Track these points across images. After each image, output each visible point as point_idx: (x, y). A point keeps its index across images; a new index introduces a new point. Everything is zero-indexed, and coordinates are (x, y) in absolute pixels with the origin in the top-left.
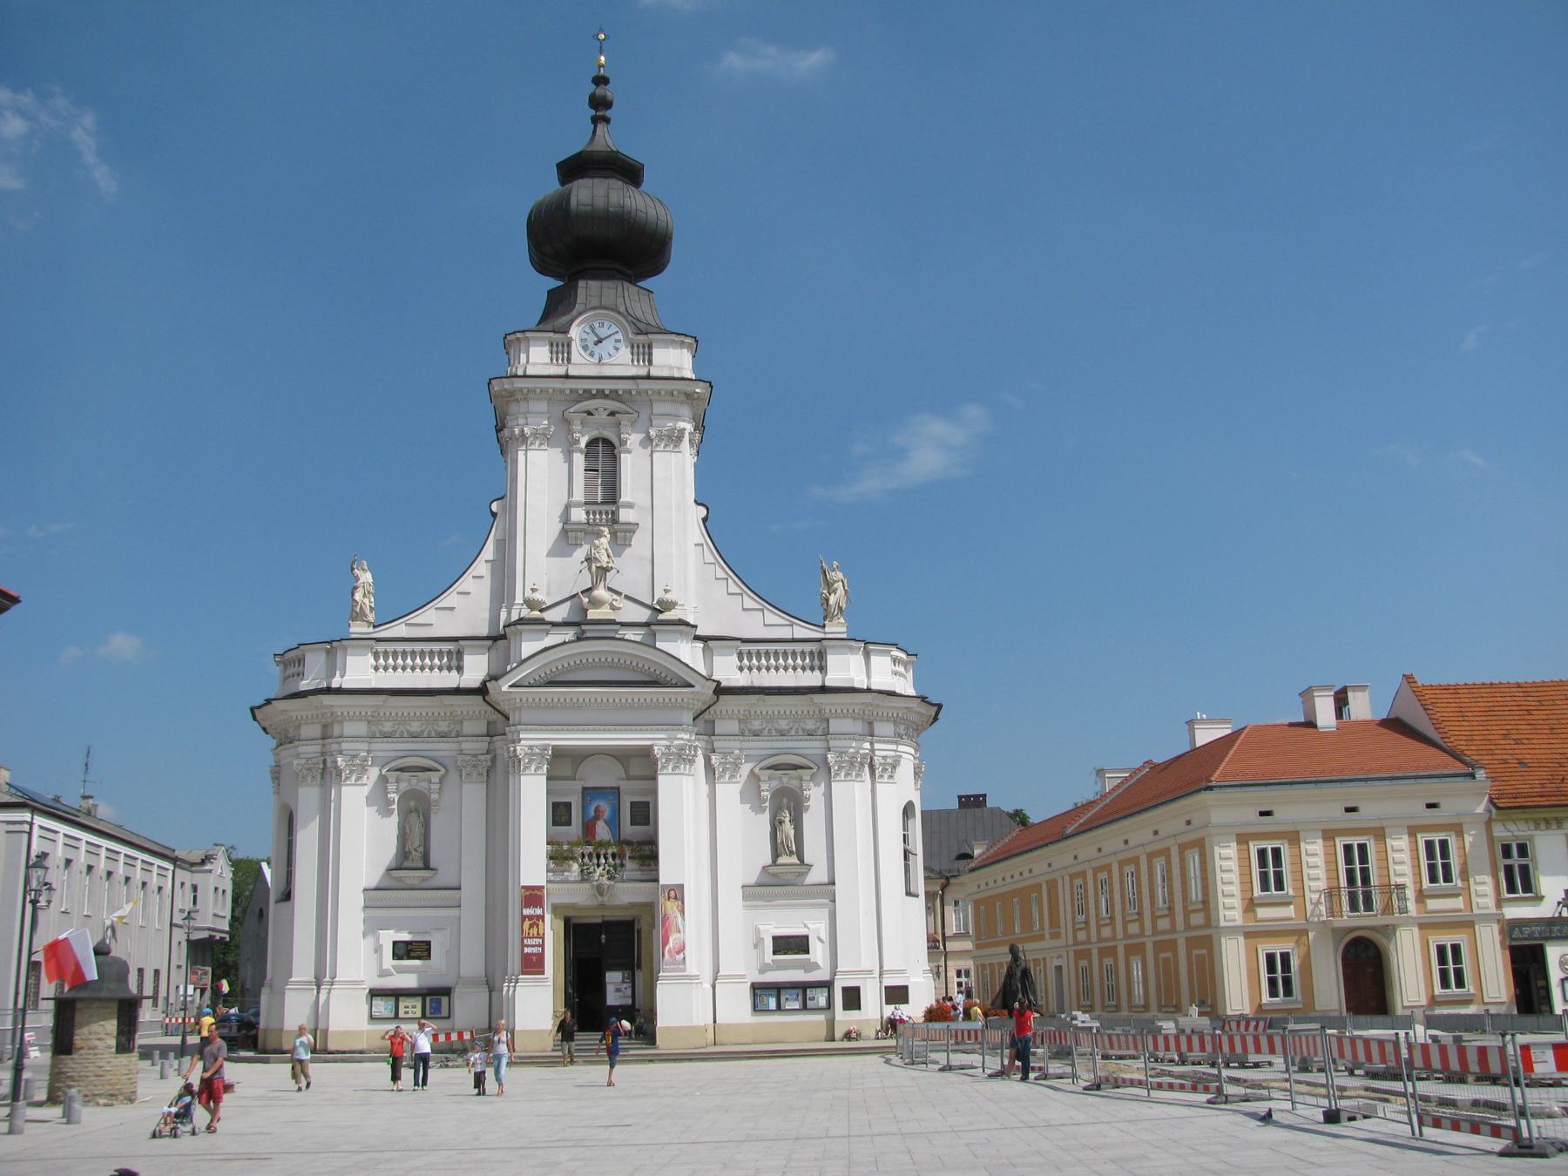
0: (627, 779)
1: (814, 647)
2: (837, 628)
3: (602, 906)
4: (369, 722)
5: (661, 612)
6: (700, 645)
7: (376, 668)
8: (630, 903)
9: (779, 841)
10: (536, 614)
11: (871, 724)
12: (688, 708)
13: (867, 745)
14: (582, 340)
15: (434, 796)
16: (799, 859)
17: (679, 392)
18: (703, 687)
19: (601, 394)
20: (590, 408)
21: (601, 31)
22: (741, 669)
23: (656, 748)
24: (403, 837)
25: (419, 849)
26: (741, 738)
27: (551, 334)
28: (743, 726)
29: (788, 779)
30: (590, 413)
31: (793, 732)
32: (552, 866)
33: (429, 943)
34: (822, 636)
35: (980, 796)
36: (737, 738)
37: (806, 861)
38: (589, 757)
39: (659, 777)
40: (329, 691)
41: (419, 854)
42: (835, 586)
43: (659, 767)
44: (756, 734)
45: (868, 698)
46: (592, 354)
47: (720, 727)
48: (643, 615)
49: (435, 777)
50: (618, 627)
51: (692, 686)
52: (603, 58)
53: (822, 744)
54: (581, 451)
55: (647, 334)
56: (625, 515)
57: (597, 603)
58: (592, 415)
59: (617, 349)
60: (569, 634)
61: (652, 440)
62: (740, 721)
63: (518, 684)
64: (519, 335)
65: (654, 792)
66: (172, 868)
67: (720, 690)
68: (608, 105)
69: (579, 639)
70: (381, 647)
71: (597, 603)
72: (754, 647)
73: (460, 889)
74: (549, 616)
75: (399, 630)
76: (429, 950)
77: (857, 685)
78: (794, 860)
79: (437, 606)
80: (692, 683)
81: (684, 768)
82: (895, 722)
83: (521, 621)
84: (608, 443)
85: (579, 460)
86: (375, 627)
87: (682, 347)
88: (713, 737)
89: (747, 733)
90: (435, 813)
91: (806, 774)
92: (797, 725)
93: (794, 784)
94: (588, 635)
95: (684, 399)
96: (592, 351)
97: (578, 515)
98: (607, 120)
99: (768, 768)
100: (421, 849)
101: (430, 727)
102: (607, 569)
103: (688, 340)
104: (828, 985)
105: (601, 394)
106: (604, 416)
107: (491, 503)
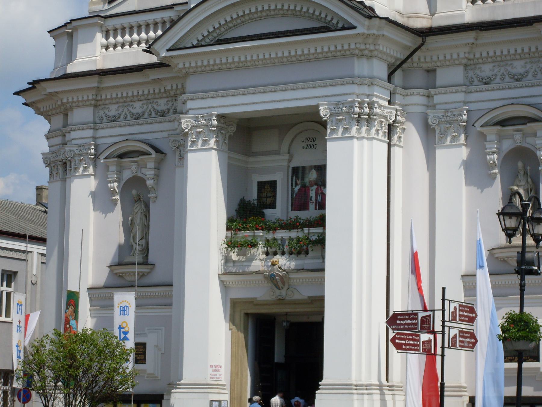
3: (280, 301)
4: (95, 106)
7: (107, 48)
8: (309, 297)
15: (149, 183)
18: (369, 28)
24: (128, 228)
26: (464, 88)
28: (471, 74)
32: (234, 256)
36: (459, 88)
39: (329, 144)
40: (67, 77)
49: (150, 162)
62: (466, 66)
63: (174, 48)
73: (172, 285)
80: (355, 25)
81: (359, 131)
88: (432, 91)
89: (476, 82)
90: (154, 202)
92: (535, 66)
93: (529, 142)
101: (126, 110)
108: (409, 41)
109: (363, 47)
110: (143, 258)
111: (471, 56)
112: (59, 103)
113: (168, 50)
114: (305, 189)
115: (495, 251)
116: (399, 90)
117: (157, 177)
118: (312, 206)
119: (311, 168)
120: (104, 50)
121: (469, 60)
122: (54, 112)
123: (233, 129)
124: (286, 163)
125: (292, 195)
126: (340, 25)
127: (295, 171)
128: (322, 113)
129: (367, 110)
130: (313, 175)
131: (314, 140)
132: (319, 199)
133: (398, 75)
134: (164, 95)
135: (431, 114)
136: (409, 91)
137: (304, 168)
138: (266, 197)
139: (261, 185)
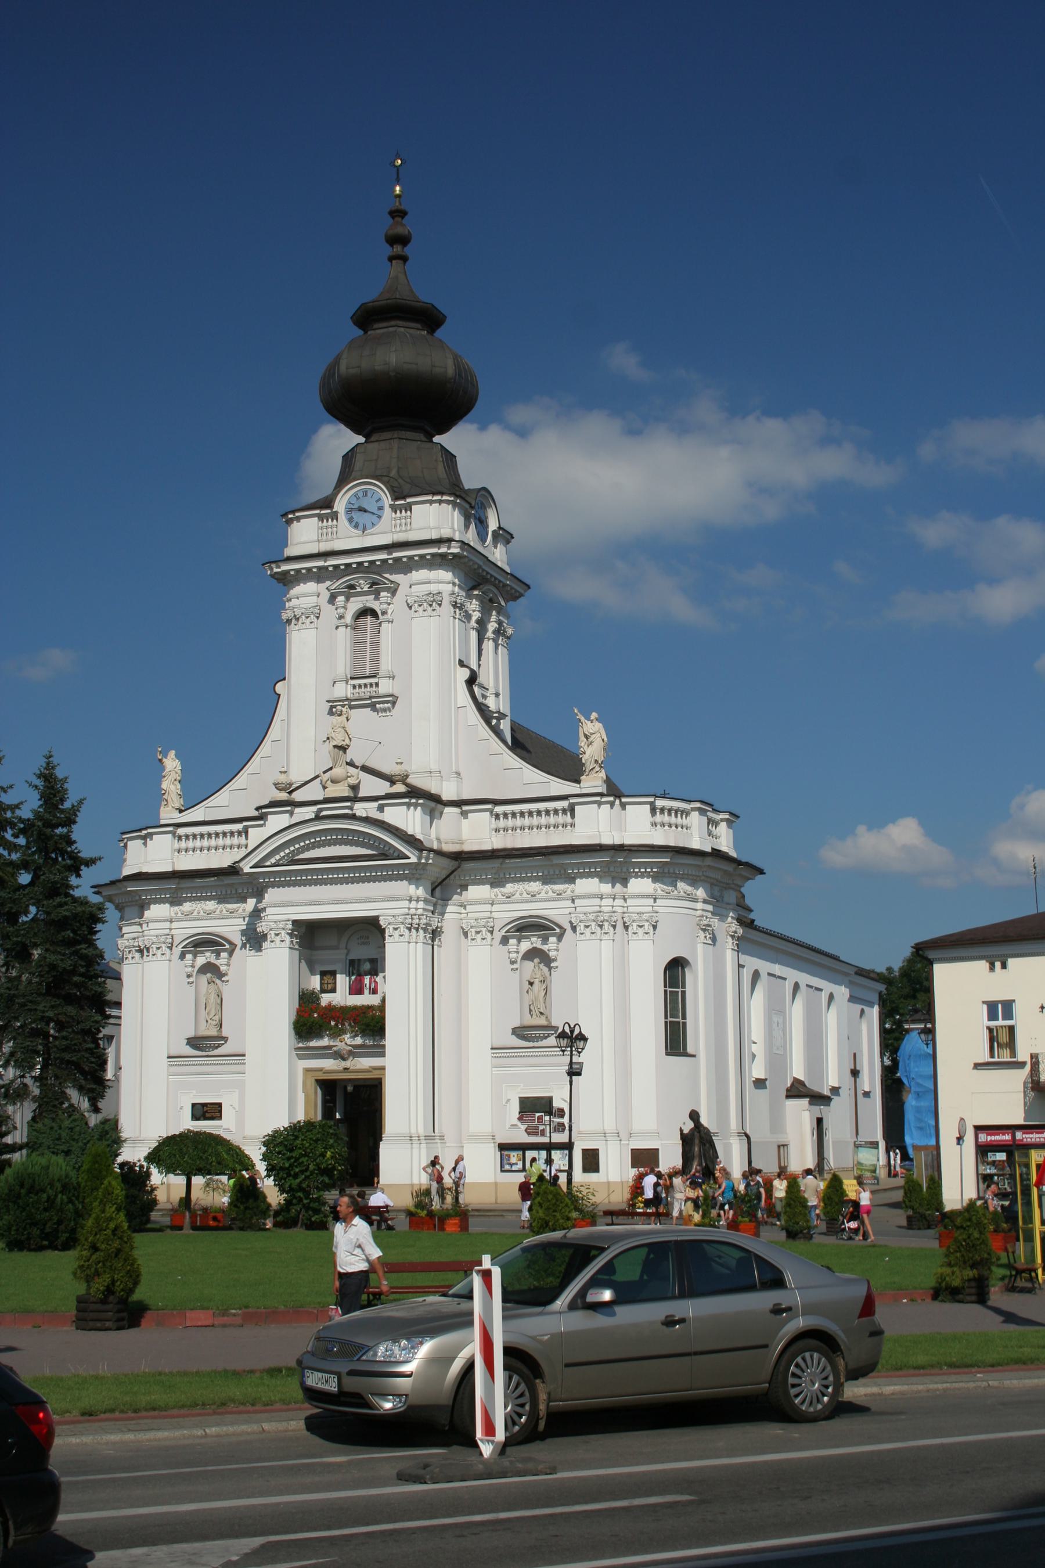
2: (593, 782)
5: (393, 783)
6: (455, 810)
7: (179, 851)
10: (283, 796)
14: (349, 511)
16: (546, 1021)
17: (433, 555)
18: (420, 858)
20: (352, 582)
21: (398, 157)
22: (497, 830)
23: (381, 918)
25: (214, 1018)
29: (534, 941)
30: (352, 587)
33: (220, 1105)
34: (578, 791)
38: (354, 925)
41: (214, 1023)
42: (593, 737)
43: (387, 935)
46: (356, 526)
48: (382, 787)
50: (348, 804)
51: (409, 858)
52: (398, 188)
54: (347, 626)
55: (404, 498)
60: (309, 812)
61: (410, 608)
64: (290, 516)
67: (460, 857)
68: (403, 240)
69: (318, 818)
70: (181, 831)
74: (298, 796)
75: (197, 814)
76: (220, 1111)
77: (607, 840)
79: (230, 789)
83: (273, 804)
84: (373, 613)
85: (344, 635)
86: (181, 811)
87: (444, 505)
95: (440, 560)
96: (357, 523)
97: (342, 690)
98: (404, 259)
100: (217, 1018)
102: (343, 749)
103: (445, 498)
104: (569, 1146)
106: (366, 589)
107: (277, 683)
108: (448, 864)
109: (415, 872)
110: (217, 1031)
111: (497, 876)
112: (137, 898)
113: (251, 868)
115: (516, 1030)
116: (440, 902)
117: (228, 965)
118: (366, 991)
119: (365, 960)
120: (176, 853)
121: (495, 879)
122: (129, 904)
123: (303, 930)
124: (343, 957)
125: (350, 982)
126: (396, 854)
128: (381, 923)
131: (368, 938)
132: (373, 986)
133: (438, 890)
134: (235, 896)
137: (359, 960)
138: (328, 984)
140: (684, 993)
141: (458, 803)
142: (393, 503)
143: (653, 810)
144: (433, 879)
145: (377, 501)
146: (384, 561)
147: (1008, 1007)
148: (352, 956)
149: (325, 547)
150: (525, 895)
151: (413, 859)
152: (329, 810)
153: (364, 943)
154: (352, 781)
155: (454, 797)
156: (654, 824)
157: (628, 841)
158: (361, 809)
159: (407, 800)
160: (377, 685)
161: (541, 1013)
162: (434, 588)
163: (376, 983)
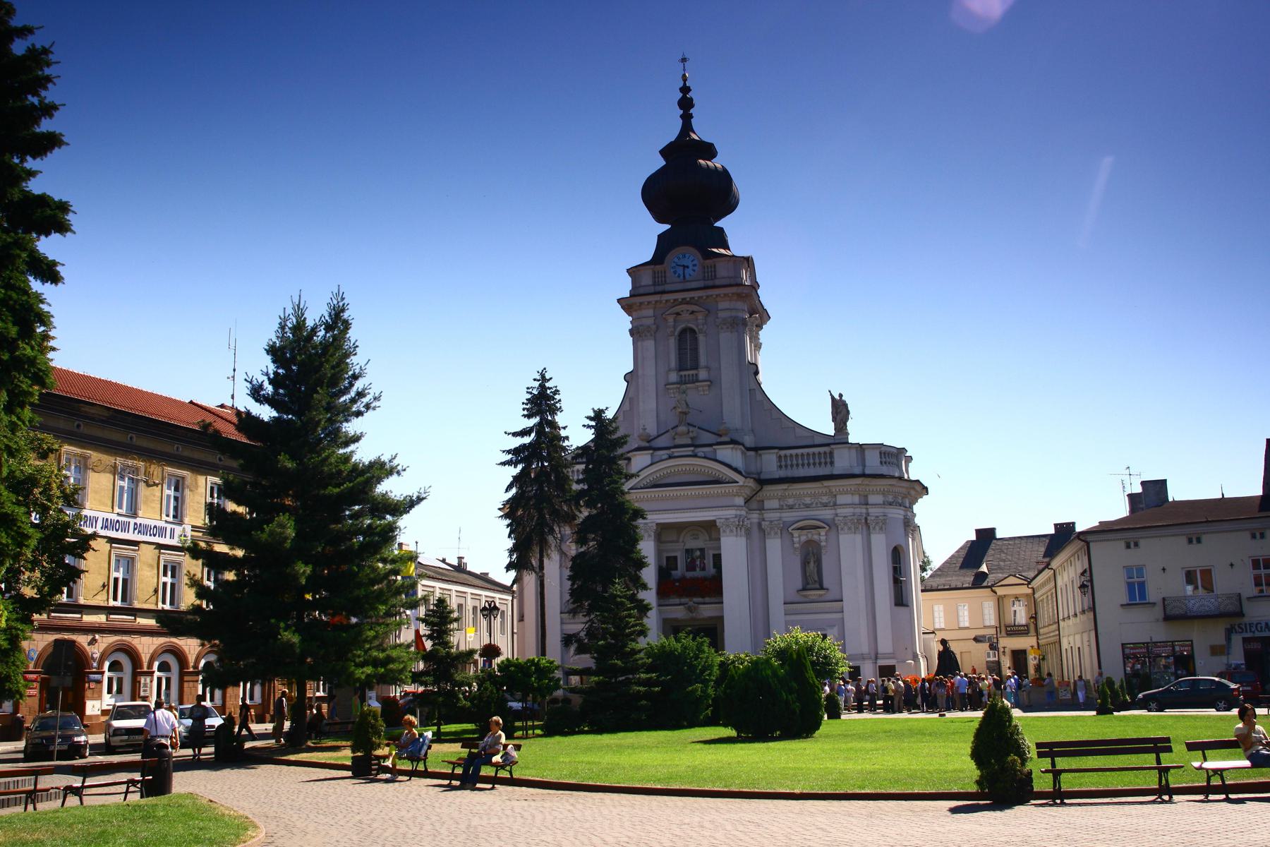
0: (710, 540)
1: (826, 449)
3: (693, 619)
6: (752, 453)
9: (808, 574)
11: (866, 497)
12: (739, 496)
13: (864, 511)
17: (733, 294)
18: (744, 483)
19: (684, 302)
20: (679, 311)
23: (718, 521)
27: (652, 266)
30: (678, 314)
31: (814, 505)
35: (1070, 523)
37: (825, 586)
38: (687, 527)
39: (722, 539)
43: (721, 531)
44: (791, 507)
45: (858, 481)
47: (767, 504)
50: (692, 449)
51: (737, 482)
53: (833, 511)
56: (703, 374)
57: (681, 435)
58: (680, 315)
59: (694, 271)
60: (663, 454)
62: (779, 499)
65: (719, 548)
66: (510, 598)
69: (670, 457)
71: (681, 435)
72: (788, 452)
78: (817, 586)
80: (737, 480)
82: (883, 494)
84: (692, 331)
85: (672, 342)
88: (763, 512)
89: (785, 507)
91: (823, 532)
92: (816, 500)
93: (816, 537)
94: (676, 454)
99: (798, 529)
105: (684, 302)
114: (693, 561)
118: (698, 569)
126: (727, 480)
127: (688, 551)
129: (741, 523)
130: (698, 553)
132: (702, 565)
133: (747, 505)
135: (763, 523)
136: (751, 512)
137: (692, 550)
139: (668, 558)
140: (900, 567)
141: (756, 449)
142: (702, 260)
143: (880, 453)
144: (746, 496)
145: (692, 261)
146: (700, 298)
147: (1140, 570)
148: (688, 546)
149: (660, 288)
150: (802, 506)
151: (741, 483)
152: (677, 452)
153: (695, 538)
154: (694, 434)
155: (753, 446)
156: (881, 463)
157: (867, 472)
158: (700, 451)
159: (731, 446)
160: (696, 375)
161: (815, 581)
162: (734, 314)
163: (704, 564)
